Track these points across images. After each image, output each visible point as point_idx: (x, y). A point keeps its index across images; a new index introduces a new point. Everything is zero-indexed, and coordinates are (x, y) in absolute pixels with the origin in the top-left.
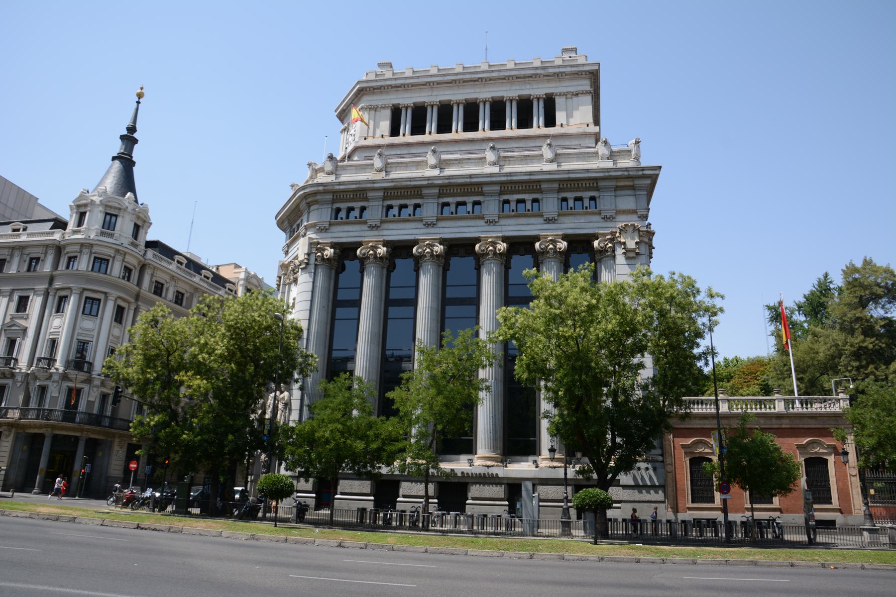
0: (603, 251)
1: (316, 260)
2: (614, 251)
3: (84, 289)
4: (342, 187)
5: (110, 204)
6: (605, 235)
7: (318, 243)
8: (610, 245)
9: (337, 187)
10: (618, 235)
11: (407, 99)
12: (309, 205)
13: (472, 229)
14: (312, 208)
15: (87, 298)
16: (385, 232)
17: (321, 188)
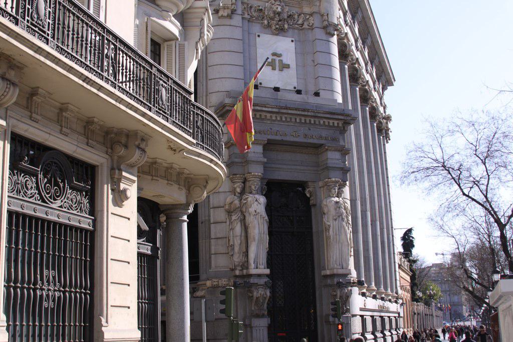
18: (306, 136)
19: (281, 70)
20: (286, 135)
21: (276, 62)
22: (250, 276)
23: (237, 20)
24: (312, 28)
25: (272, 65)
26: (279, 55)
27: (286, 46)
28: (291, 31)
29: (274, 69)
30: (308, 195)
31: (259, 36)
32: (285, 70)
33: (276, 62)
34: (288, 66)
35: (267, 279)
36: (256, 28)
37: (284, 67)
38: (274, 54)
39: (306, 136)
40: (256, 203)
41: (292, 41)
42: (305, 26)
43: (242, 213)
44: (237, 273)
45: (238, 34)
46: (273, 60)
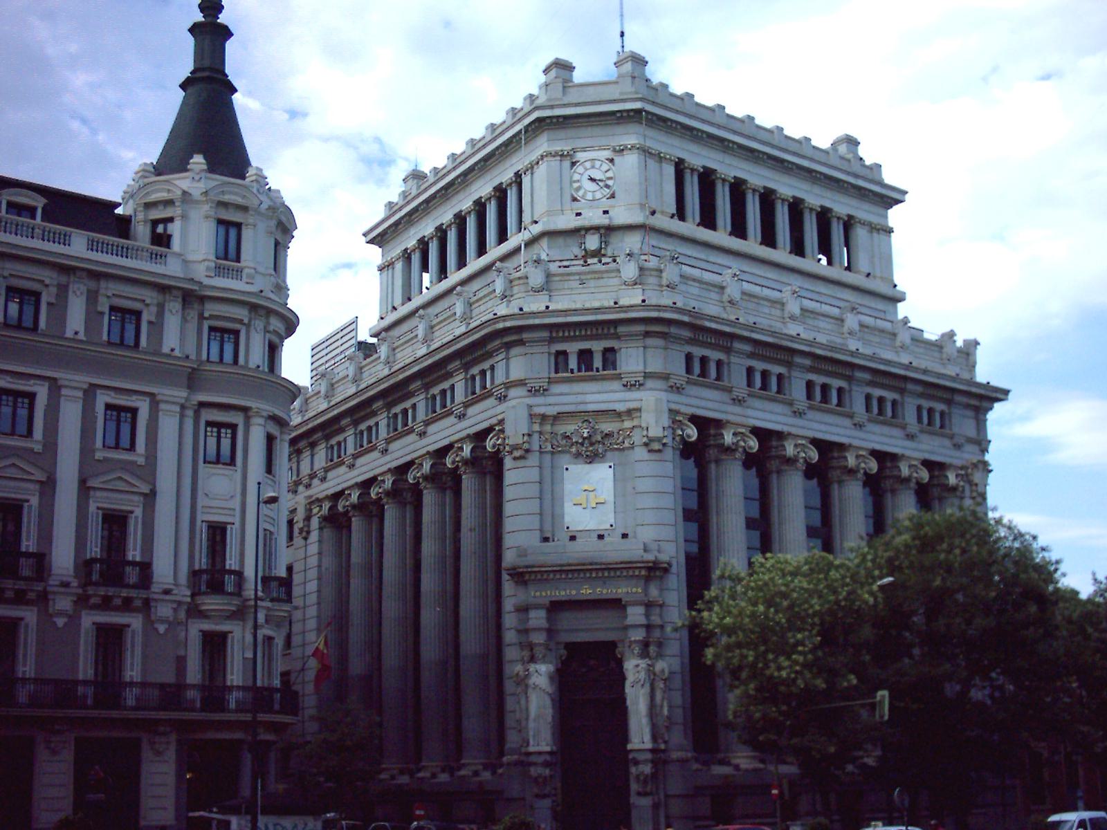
0: (954, 489)
1: (674, 439)
2: (963, 491)
3: (202, 405)
4: (714, 326)
5: (226, 198)
6: (956, 468)
7: (678, 412)
8: (962, 483)
9: (708, 324)
10: (970, 471)
11: (699, 157)
12: (647, 334)
13: (834, 430)
14: (650, 341)
15: (209, 424)
16: (749, 412)
17: (686, 319)
22: (529, 754)
23: (533, 459)
24: (632, 447)
30: (619, 656)
31: (567, 469)
35: (548, 758)
36: (564, 461)
40: (536, 674)
41: (610, 467)
42: (626, 444)
43: (527, 686)
44: (523, 750)
45: (534, 474)
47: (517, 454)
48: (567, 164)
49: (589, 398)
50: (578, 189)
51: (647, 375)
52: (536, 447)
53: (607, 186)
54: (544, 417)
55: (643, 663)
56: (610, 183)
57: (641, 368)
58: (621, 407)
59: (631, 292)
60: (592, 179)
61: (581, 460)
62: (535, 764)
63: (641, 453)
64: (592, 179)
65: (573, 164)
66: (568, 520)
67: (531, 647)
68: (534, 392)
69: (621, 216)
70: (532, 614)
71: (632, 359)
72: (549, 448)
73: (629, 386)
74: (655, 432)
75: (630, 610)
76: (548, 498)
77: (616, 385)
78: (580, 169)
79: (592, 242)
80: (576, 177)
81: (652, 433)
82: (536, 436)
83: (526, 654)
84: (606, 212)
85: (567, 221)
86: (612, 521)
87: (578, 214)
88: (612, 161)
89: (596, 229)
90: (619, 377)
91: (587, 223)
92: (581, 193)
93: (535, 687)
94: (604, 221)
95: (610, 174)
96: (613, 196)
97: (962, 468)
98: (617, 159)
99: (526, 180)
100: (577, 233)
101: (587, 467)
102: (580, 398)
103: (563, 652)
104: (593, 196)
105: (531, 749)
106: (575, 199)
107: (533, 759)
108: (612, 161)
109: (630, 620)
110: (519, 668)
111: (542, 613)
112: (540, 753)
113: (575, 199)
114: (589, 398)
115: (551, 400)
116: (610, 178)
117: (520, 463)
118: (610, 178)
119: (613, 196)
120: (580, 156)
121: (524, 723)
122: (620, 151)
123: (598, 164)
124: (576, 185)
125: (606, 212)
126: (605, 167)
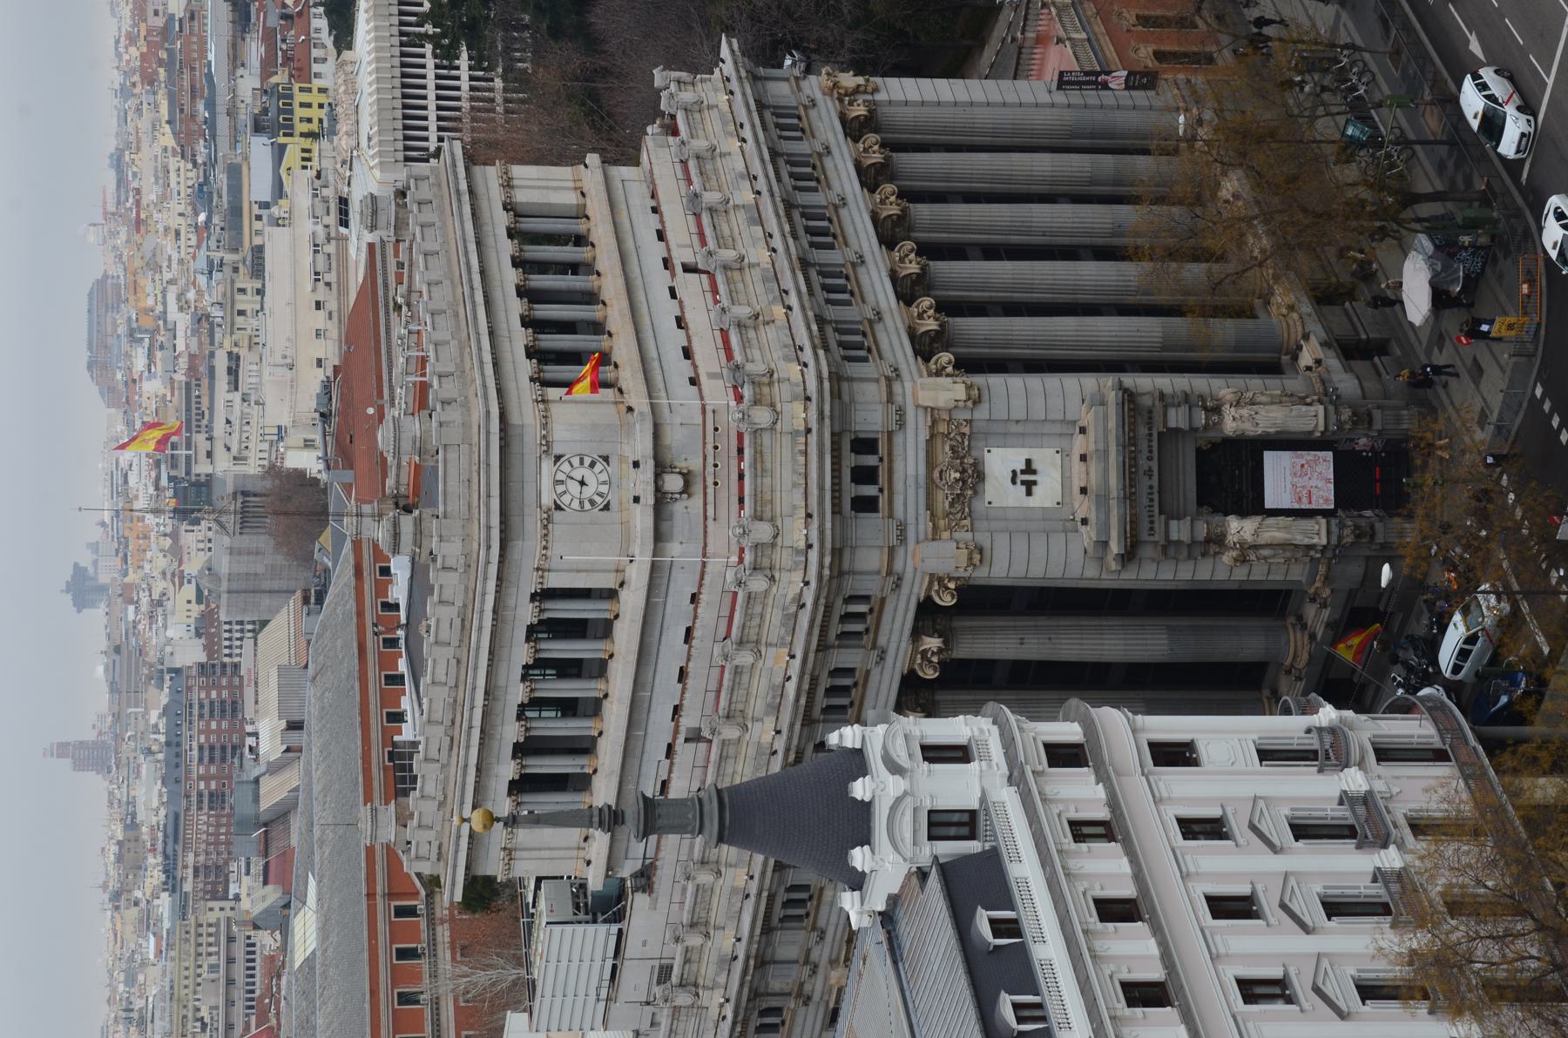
14: (846, 398)
18: (1150, 459)
19: (1034, 472)
20: (1151, 487)
21: (1027, 477)
25: (1029, 486)
26: (1014, 472)
27: (1000, 462)
28: (974, 453)
29: (1034, 483)
32: (1034, 466)
33: (1027, 477)
34: (1028, 462)
36: (978, 506)
37: (1029, 468)
38: (1014, 482)
39: (1150, 459)
42: (966, 430)
46: (1023, 483)
47: (977, 557)
48: (557, 515)
49: (911, 471)
50: (592, 502)
51: (890, 399)
52: (969, 535)
53: (592, 465)
54: (935, 528)
55: (1229, 413)
56: (587, 461)
57: (879, 407)
58: (924, 435)
59: (786, 417)
60: (582, 483)
61: (979, 488)
62: (1340, 538)
63: (981, 413)
64: (582, 483)
65: (558, 508)
66: (1048, 504)
67: (1208, 541)
68: (902, 539)
69: (641, 445)
70: (1174, 536)
71: (870, 418)
72: (967, 522)
73: (901, 423)
74: (959, 392)
75: (1172, 424)
76: (1024, 525)
77: (898, 439)
78: (566, 499)
79: (673, 483)
80: (576, 505)
81: (963, 396)
82: (957, 535)
83: (1213, 548)
84: (636, 464)
85: (642, 519)
86: (1053, 451)
87: (636, 500)
88: (558, 458)
89: (658, 476)
90: (890, 434)
91: (651, 488)
92: (598, 500)
93: (1256, 533)
94: (648, 468)
95: (576, 462)
96: (606, 459)
97: (841, 101)
98: (557, 450)
99: (555, 581)
100: (661, 500)
101: (988, 480)
102: (911, 482)
103: (1205, 509)
104: (604, 483)
105: (1324, 542)
106: (607, 507)
107: (1334, 540)
108: (558, 458)
109: (1183, 425)
110: (1227, 558)
111: (1174, 524)
112: (1329, 533)
113: (607, 507)
114: (911, 471)
115: (911, 519)
116: (582, 462)
117: (987, 553)
118: (582, 462)
119: (606, 459)
120: (547, 500)
121: (1288, 554)
122: (547, 444)
123: (560, 476)
124: (587, 506)
125: (636, 464)
126: (566, 467)
